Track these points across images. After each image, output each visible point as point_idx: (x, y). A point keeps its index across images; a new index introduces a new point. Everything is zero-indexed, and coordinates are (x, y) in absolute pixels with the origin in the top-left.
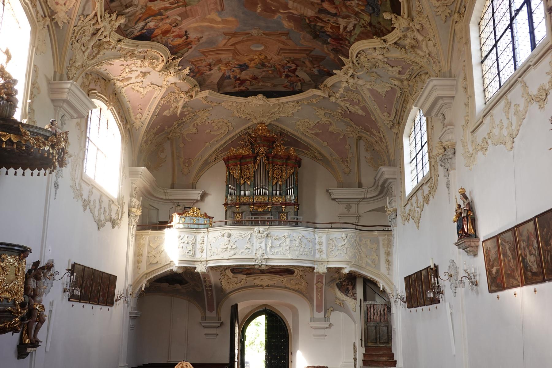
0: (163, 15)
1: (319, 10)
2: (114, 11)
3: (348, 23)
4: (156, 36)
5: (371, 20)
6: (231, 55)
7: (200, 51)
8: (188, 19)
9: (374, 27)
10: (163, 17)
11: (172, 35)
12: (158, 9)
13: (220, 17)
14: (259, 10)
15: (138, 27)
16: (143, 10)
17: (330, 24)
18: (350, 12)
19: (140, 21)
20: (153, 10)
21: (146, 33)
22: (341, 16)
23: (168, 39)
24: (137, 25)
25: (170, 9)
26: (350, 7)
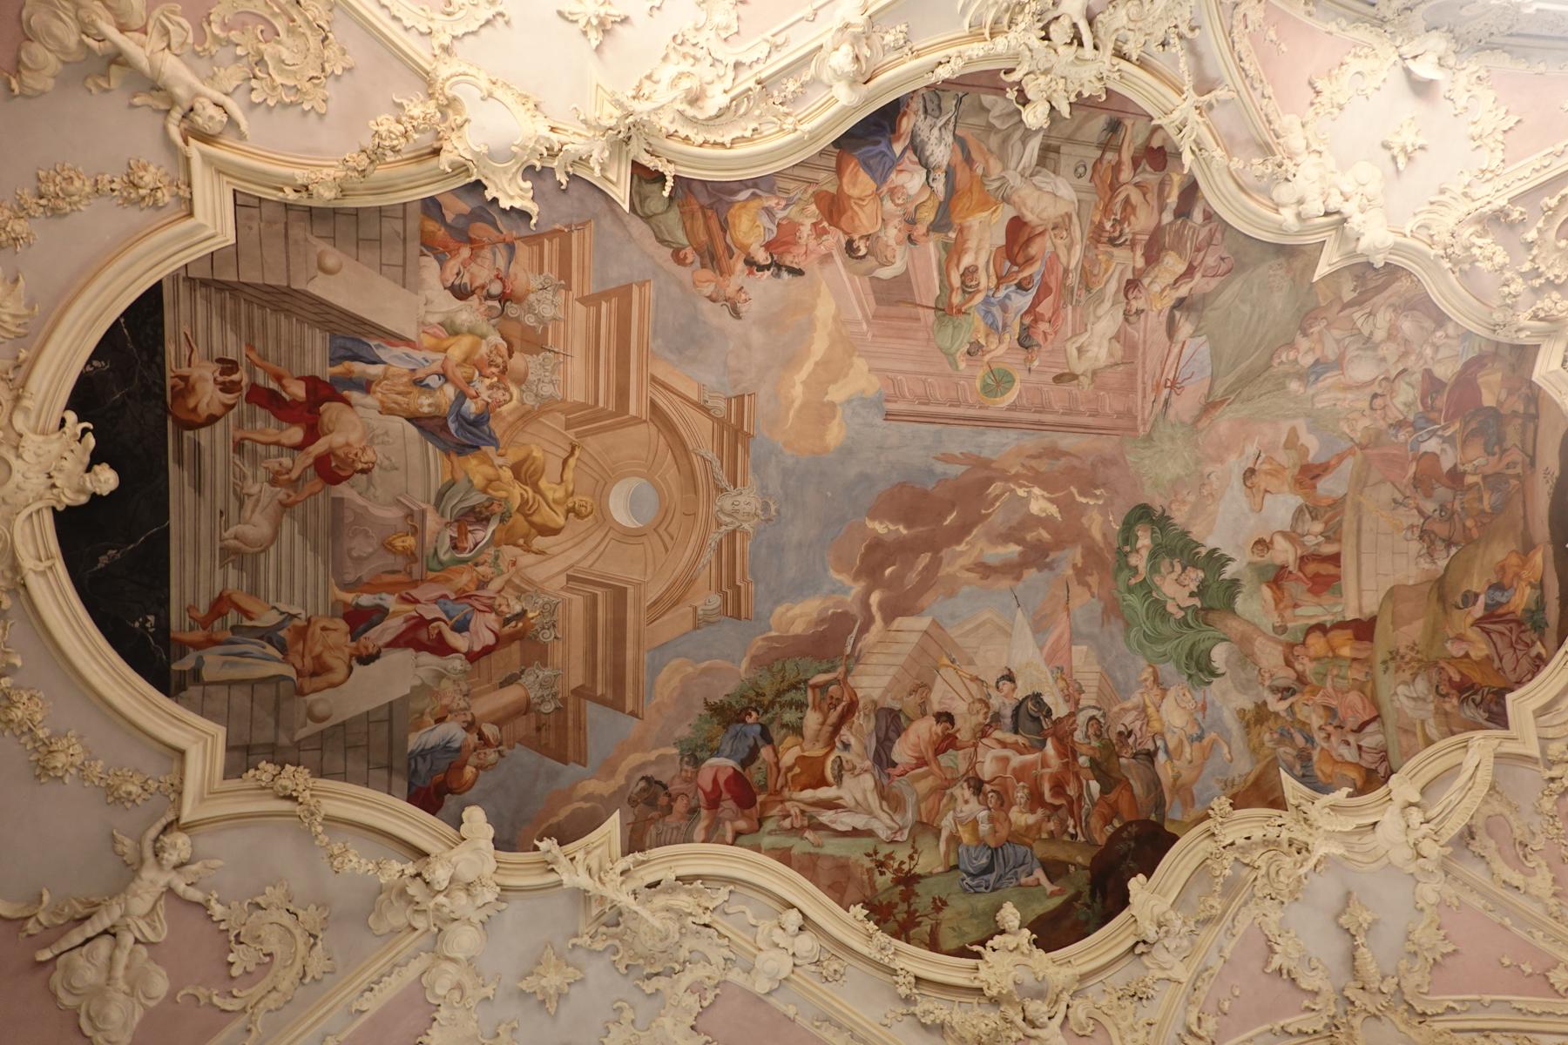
0: (928, 231)
1: (891, 711)
2: (1074, 113)
3: (859, 807)
4: (839, 171)
5: (931, 875)
6: (577, 395)
7: (642, 285)
8: (871, 298)
9: (907, 897)
10: (921, 229)
11: (808, 223)
12: (970, 227)
13: (849, 401)
14: (880, 528)
15: (941, 139)
16: (997, 184)
17: (827, 754)
18: (923, 806)
19: (959, 157)
20: (971, 211)
21: (882, 147)
22: (885, 781)
23: (788, 199)
24: (949, 139)
25: (948, 261)
26: (945, 801)
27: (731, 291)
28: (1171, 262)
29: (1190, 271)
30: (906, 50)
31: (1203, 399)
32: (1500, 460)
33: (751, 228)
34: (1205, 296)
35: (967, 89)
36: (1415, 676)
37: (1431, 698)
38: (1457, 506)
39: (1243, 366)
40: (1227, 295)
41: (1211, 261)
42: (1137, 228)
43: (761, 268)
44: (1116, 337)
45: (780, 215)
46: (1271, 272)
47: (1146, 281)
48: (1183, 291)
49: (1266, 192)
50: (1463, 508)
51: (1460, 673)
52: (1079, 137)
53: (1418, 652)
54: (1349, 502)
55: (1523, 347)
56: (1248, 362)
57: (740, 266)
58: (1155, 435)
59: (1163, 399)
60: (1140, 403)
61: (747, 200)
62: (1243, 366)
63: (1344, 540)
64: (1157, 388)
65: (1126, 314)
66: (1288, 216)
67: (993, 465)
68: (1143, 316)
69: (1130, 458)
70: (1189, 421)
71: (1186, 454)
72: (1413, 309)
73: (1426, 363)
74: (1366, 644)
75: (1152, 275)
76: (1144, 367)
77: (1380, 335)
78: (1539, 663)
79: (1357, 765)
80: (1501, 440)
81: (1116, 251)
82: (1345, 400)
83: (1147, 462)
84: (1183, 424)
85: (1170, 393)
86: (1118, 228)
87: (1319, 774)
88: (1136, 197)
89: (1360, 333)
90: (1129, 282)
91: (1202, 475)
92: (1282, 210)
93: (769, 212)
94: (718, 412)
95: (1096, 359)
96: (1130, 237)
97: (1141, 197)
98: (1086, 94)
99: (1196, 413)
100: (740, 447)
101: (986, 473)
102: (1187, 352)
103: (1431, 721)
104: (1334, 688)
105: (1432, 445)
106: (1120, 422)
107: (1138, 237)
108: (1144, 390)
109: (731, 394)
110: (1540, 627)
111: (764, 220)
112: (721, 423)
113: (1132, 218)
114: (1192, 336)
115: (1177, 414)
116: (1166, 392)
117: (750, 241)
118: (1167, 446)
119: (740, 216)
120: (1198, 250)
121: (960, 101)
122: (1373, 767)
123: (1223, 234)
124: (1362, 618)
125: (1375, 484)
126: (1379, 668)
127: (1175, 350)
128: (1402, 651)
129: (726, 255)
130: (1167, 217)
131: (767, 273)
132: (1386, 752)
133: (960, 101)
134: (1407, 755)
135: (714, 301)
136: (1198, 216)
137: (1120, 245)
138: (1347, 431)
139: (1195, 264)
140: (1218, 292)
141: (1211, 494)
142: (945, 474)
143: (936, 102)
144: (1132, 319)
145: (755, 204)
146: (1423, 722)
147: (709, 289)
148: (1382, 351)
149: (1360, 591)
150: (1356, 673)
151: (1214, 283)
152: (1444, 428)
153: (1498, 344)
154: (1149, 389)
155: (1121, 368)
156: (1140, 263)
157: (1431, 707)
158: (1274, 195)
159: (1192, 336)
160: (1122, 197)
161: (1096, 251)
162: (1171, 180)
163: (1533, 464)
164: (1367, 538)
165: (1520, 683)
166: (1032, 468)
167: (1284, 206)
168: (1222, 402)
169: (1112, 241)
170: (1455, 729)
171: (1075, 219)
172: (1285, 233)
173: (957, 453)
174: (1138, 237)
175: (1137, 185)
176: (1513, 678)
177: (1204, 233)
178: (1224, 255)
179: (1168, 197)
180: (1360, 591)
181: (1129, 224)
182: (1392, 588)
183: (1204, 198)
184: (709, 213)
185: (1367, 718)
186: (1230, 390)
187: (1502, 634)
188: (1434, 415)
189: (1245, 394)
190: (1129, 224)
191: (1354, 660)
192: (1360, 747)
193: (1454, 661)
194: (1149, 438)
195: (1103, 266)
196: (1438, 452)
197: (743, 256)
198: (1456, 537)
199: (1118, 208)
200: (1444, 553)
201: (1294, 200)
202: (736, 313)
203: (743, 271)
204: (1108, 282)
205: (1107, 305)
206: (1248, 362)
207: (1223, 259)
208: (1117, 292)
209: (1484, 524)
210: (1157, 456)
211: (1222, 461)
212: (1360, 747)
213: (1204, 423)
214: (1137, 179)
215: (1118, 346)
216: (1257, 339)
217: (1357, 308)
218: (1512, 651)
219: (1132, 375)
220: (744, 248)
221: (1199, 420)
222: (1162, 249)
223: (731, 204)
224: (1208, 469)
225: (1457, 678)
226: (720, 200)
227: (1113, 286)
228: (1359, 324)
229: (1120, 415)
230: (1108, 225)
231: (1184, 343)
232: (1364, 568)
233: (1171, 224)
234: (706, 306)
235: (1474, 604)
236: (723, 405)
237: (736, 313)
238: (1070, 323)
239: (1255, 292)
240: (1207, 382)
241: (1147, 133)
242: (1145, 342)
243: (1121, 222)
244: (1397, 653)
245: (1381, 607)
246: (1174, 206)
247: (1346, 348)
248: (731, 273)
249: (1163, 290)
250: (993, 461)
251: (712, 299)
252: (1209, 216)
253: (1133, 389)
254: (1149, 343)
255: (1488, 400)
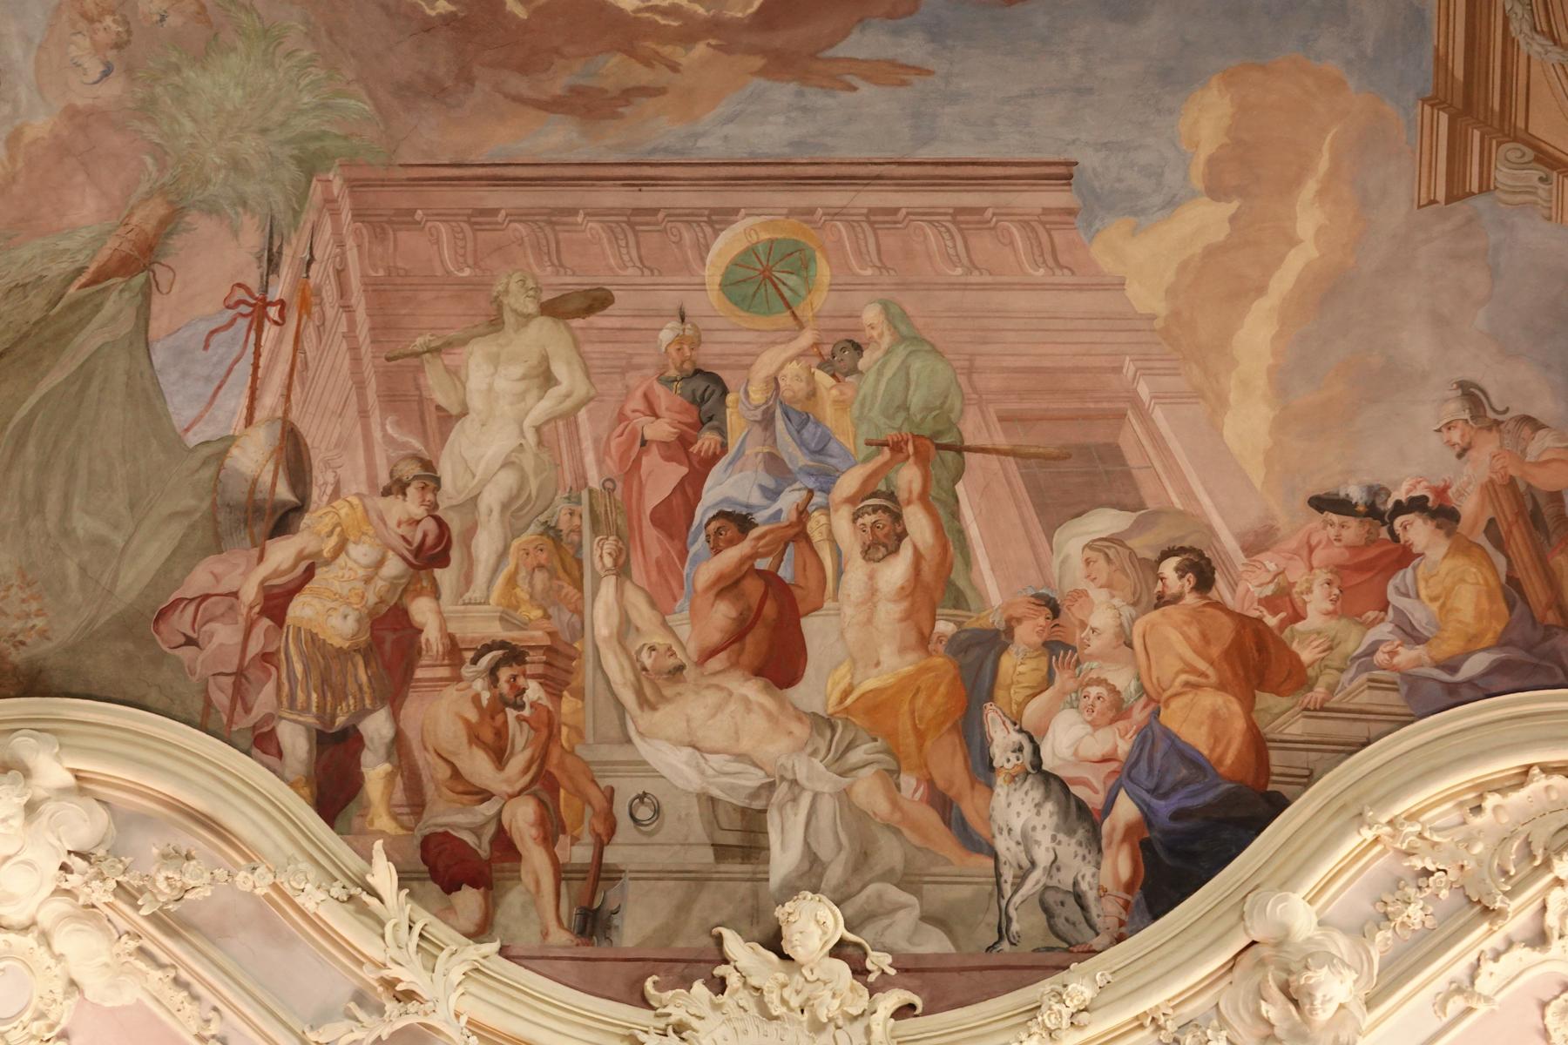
0: (1009, 632)
2: (707, 942)
4: (1258, 744)
8: (1133, 459)
10: (1029, 632)
11: (1314, 619)
12: (902, 650)
13: (1172, 204)
15: (1026, 841)
16: (856, 756)
19: (969, 808)
20: (907, 686)
21: (1164, 808)
23: (1370, 667)
24: (1002, 844)
25: (944, 566)
27: (1487, 447)
28: (336, 621)
29: (275, 603)
30: (1171, 1026)
31: (162, 275)
33: (1448, 593)
34: (217, 545)
35: (993, 959)
39: (55, 378)
40: (151, 554)
41: (224, 635)
42: (451, 692)
43: (1416, 505)
44: (448, 420)
45: (1384, 630)
46: (40, 623)
47: (394, 566)
48: (282, 554)
49: (125, 821)
52: (677, 889)
56: (44, 387)
57: (1468, 506)
58: (290, 172)
59: (286, 271)
60: (352, 256)
61: (1468, 654)
62: (55, 378)
64: (306, 299)
65: (430, 477)
66: (52, 770)
67: (758, 62)
68: (384, 479)
69: (358, 105)
70: (192, 217)
71: (189, 126)
75: (380, 584)
76: (354, 351)
81: (497, 631)
83: (307, 99)
84: (211, 209)
85: (265, 288)
86: (504, 687)
88: (479, 766)
90: (443, 560)
91: (129, 70)
92: (69, 780)
93: (1411, 635)
94: (1512, 156)
95: (495, 361)
96: (467, 671)
97: (464, 766)
98: (699, 987)
99: (176, 242)
100: (1459, 73)
101: (778, 39)
102: (234, 401)
106: (403, 200)
107: (444, 672)
108: (343, 291)
109: (1481, 203)
111: (1419, 615)
112: (1505, 128)
113: (473, 716)
114: (229, 441)
115: (236, 234)
116: (278, 290)
117: (1445, 567)
118: (249, 145)
119: (1479, 616)
120: (266, 657)
121: (1002, 932)
123: (208, 703)
127: (270, 400)
129: (1503, 528)
130: (377, 727)
131: (1401, 494)
133: (1002, 932)
135: (1527, 420)
136: (295, 739)
137: (488, 648)
139: (266, 622)
140: (184, 556)
141: (91, 21)
142: (897, 32)
143: (1060, 923)
144: (410, 470)
145: (1449, 647)
147: (1541, 445)
151: (200, 579)
154: (330, 293)
155: (419, 342)
156: (422, 610)
158: (102, 815)
159: (229, 441)
160: (517, 763)
161: (554, 625)
162: (395, 817)
166: (648, 63)
167: (64, 791)
168: (101, 276)
169: (513, 654)
171: (628, 698)
172: (42, 727)
173: (866, 90)
174: (444, 672)
175: (484, 795)
177: (264, 700)
178: (186, 653)
179: (390, 777)
181: (476, 699)
183: (292, 785)
184: (1551, 617)
186: (83, 310)
189: (38, 301)
190: (476, 699)
194: (310, 165)
195: (522, 593)
197: (1463, 527)
199: (519, 736)
201: (48, 808)
202: (1472, 395)
203: (1461, 494)
204: (503, 555)
205: (491, 498)
206: (44, 387)
207: (190, 642)
208: (470, 532)
210: (276, 116)
211: (72, 113)
213: (147, 216)
214: (488, 809)
215: (440, 398)
216: (31, 450)
219: (383, 328)
220: (1462, 547)
221: (163, 222)
222: (370, 651)
223: (1502, 642)
224: (114, 88)
226: (1529, 648)
227: (486, 545)
229: (405, 218)
230: (534, 691)
231: (249, 420)
233: (363, 713)
234: (1542, 407)
236: (1502, 175)
237: (1472, 395)
238: (587, 444)
239: (72, 568)
240: (157, 326)
241: (501, 918)
242: (364, 414)
243: (501, 703)
246: (367, 757)
248: (1489, 489)
249: (341, 548)
250: (763, 72)
251: (1531, 423)
252: (263, 743)
253: (374, 288)
254: (352, 410)
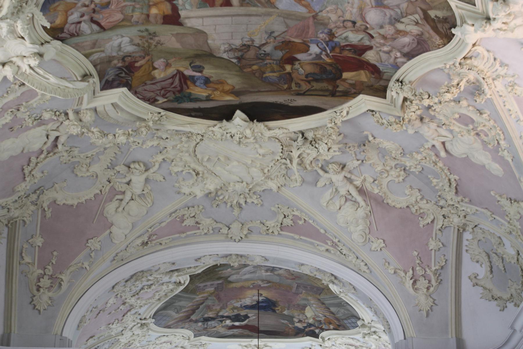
32: (302, 80)
36: (138, 45)
37: (121, 54)
38: (267, 61)
50: (266, 64)
51: (141, 66)
53: (156, 46)
54: (272, 10)
55: (385, 91)
63: (242, 8)
72: (418, 43)
73: (377, 47)
74: (162, 21)
77: (400, 27)
78: (152, 101)
79: (66, 22)
80: (316, 80)
82: (352, 7)
87: (56, 4)
89: (403, 17)
103: (103, 55)
104: (126, 6)
105: (314, 49)
110: (178, 100)
122: (65, 30)
124: (181, 19)
125: (286, 23)
126: (143, 28)
128: (157, 39)
132: (78, 35)
134: (77, 47)
138: (328, 9)
146: (103, 51)
148: (387, 27)
149: (202, 17)
150: (136, 16)
152: (327, 55)
153: (389, 80)
157: (114, 54)
163: (298, 94)
164: (245, 19)
165: (135, 93)
170: (98, 67)
176: (140, 89)
180: (202, 17)
182: (205, 33)
185: (103, 24)
187: (172, 83)
188: (338, 50)
191: (148, 16)
192: (80, 23)
193: (150, 63)
196: (309, 52)
198: (244, 62)
200: (232, 56)
209: (254, 74)
212: (80, 23)
217: (422, 17)
218: (159, 88)
225: (137, 65)
228: (410, 17)
232: (220, 19)
235: (194, 71)
244: (155, 36)
245: (190, 28)
247: (392, 9)
255: (345, 75)
